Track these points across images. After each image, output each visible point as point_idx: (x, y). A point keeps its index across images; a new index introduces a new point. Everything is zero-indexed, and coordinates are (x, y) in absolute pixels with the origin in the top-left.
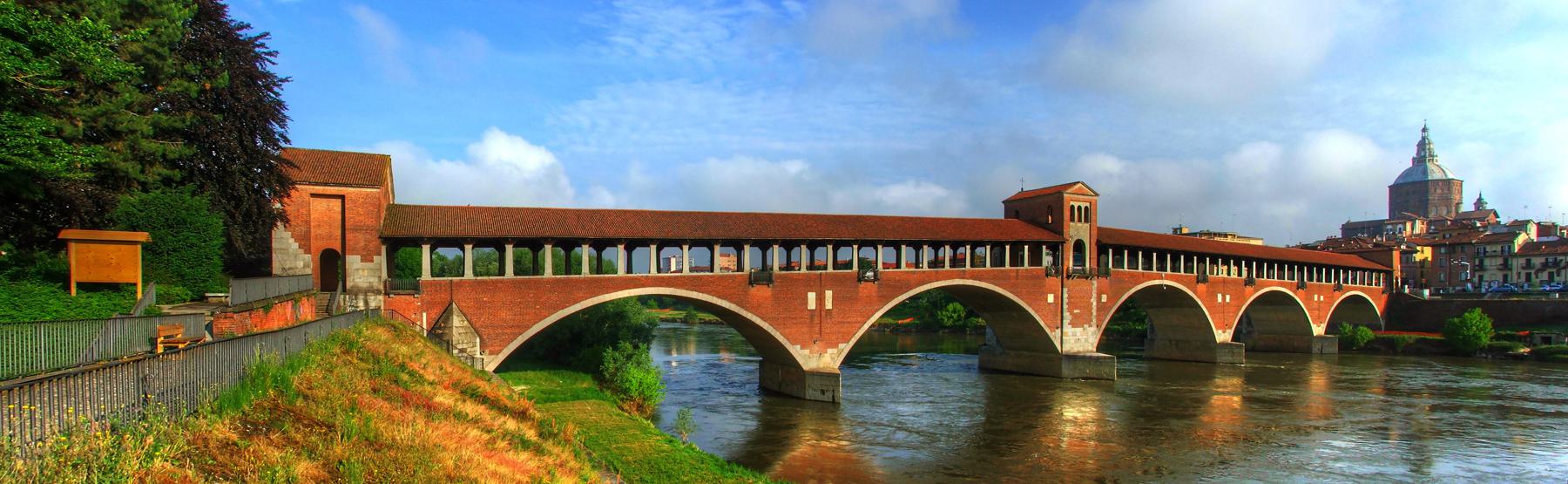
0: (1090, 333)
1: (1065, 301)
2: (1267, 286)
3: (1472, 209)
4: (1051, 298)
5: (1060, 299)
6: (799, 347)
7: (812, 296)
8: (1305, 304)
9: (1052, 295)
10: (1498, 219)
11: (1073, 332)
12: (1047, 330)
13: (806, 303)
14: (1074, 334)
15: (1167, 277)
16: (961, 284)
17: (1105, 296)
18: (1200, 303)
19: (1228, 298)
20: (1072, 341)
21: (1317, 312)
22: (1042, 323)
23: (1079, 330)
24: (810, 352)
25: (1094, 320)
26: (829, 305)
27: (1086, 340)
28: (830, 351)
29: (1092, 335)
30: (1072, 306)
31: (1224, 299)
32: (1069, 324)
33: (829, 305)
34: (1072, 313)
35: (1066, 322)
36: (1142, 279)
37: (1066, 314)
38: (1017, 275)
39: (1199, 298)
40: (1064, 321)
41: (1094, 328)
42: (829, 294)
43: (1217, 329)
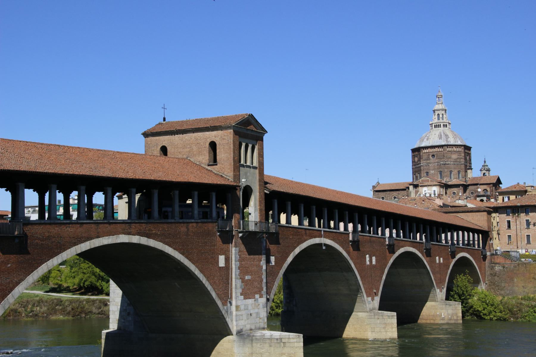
0: (261, 306)
2: (403, 247)
3: (480, 174)
8: (430, 267)
10: (500, 185)
11: (245, 305)
12: (219, 303)
14: (246, 309)
15: (327, 235)
16: (127, 241)
18: (353, 265)
19: (374, 259)
20: (245, 317)
21: (438, 276)
22: (214, 295)
23: (250, 301)
25: (265, 289)
27: (258, 313)
29: (263, 305)
30: (243, 270)
31: (371, 261)
32: (241, 294)
34: (243, 280)
36: (305, 237)
38: (188, 230)
39: (352, 259)
41: (263, 300)
43: (368, 296)
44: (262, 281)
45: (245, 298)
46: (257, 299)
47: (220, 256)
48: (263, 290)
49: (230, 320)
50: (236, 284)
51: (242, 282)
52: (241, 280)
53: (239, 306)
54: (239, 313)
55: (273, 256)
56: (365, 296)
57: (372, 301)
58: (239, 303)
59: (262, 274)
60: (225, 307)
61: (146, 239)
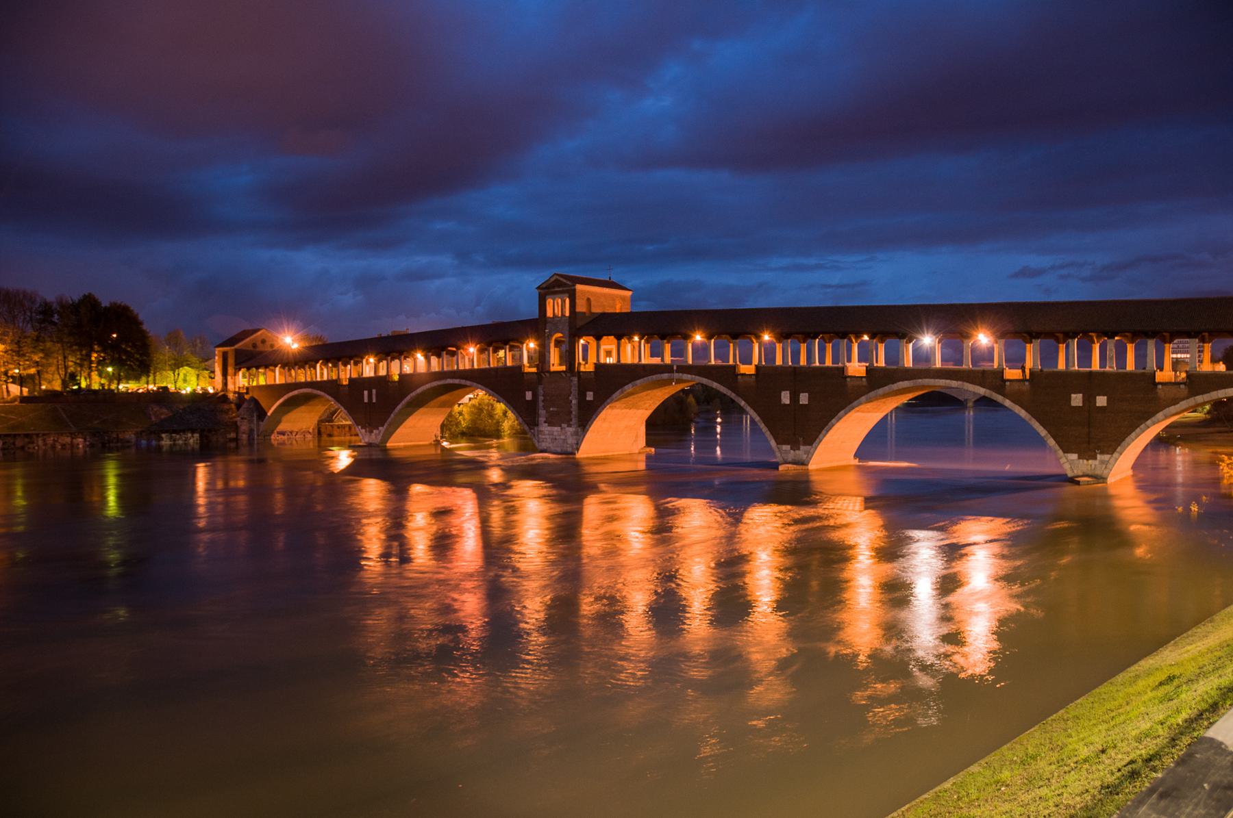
0: (569, 433)
1: (541, 398)
5: (535, 395)
6: (360, 427)
7: (366, 393)
9: (530, 392)
13: (363, 397)
14: (551, 434)
17: (591, 393)
18: (743, 403)
20: (549, 440)
23: (556, 428)
25: (574, 421)
26: (374, 401)
27: (565, 440)
28: (374, 431)
29: (572, 435)
31: (795, 398)
33: (374, 401)
35: (542, 419)
40: (540, 419)
42: (374, 391)
43: (778, 444)
44: (571, 412)
45: (549, 426)
46: (565, 428)
47: (527, 392)
49: (536, 441)
50: (542, 412)
51: (546, 412)
52: (545, 411)
53: (541, 431)
54: (543, 437)
55: (590, 391)
56: (773, 443)
57: (792, 451)
59: (571, 407)
60: (532, 431)
61: (464, 381)
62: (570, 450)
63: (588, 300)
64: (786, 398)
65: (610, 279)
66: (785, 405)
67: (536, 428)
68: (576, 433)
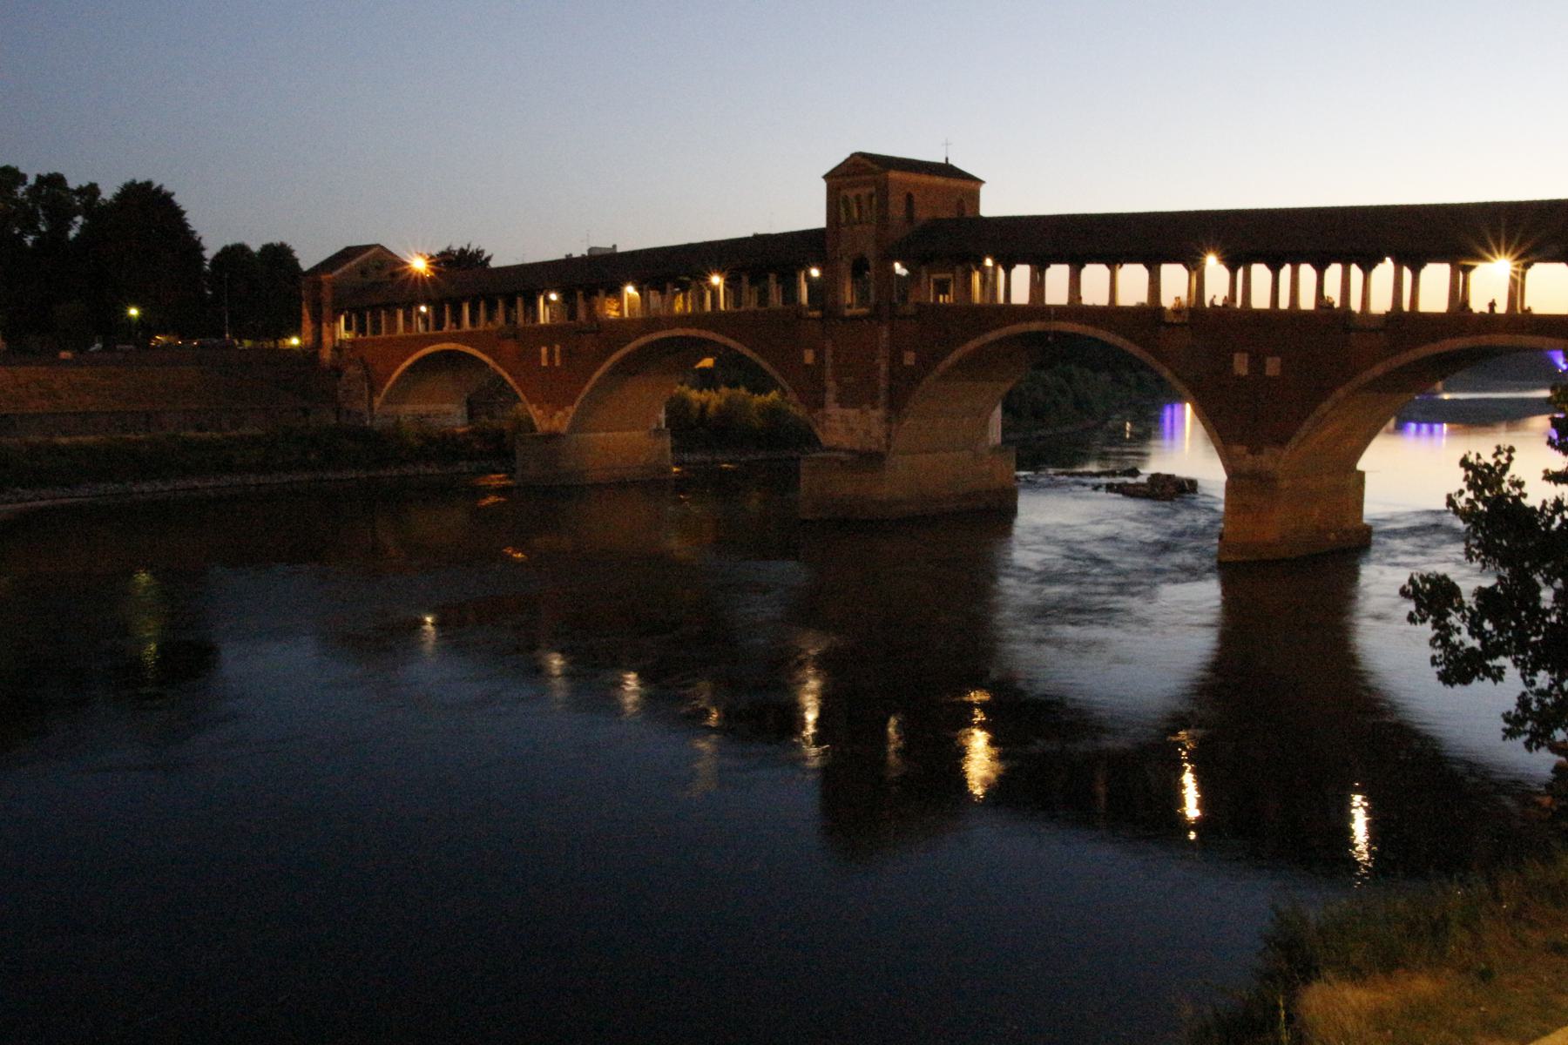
1: (829, 360)
4: (809, 356)
5: (819, 354)
6: (534, 406)
7: (544, 350)
14: (844, 420)
18: (1167, 374)
23: (852, 413)
24: (545, 413)
26: (558, 363)
27: (867, 433)
28: (560, 414)
31: (1257, 363)
33: (558, 363)
34: (839, 383)
35: (830, 397)
37: (831, 384)
41: (879, 413)
42: (557, 348)
47: (806, 351)
48: (878, 397)
57: (1249, 457)
58: (829, 411)
62: (874, 447)
63: (909, 197)
64: (1241, 364)
65: (947, 159)
66: (1239, 378)
67: (820, 412)
68: (888, 420)
